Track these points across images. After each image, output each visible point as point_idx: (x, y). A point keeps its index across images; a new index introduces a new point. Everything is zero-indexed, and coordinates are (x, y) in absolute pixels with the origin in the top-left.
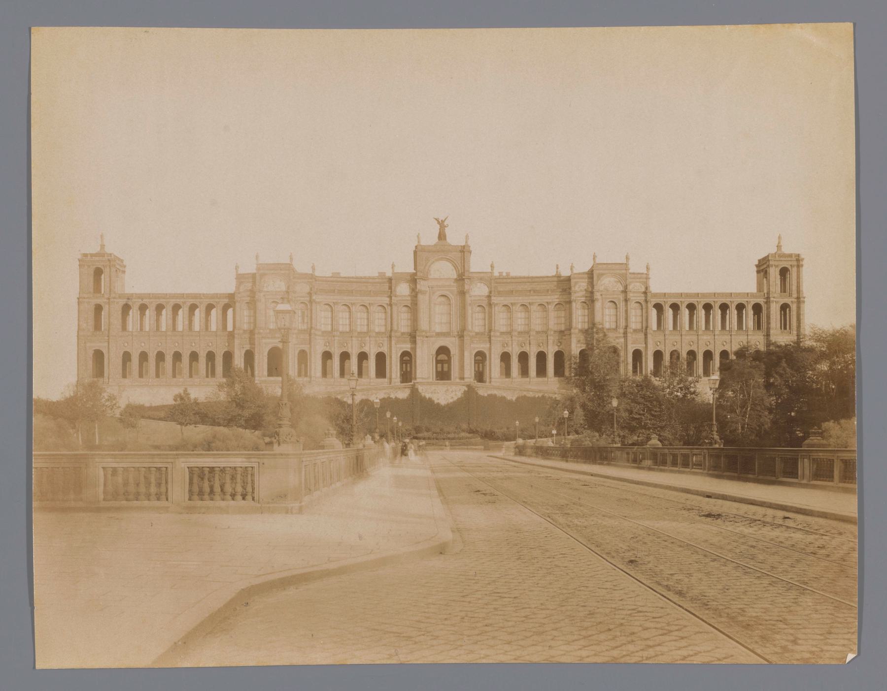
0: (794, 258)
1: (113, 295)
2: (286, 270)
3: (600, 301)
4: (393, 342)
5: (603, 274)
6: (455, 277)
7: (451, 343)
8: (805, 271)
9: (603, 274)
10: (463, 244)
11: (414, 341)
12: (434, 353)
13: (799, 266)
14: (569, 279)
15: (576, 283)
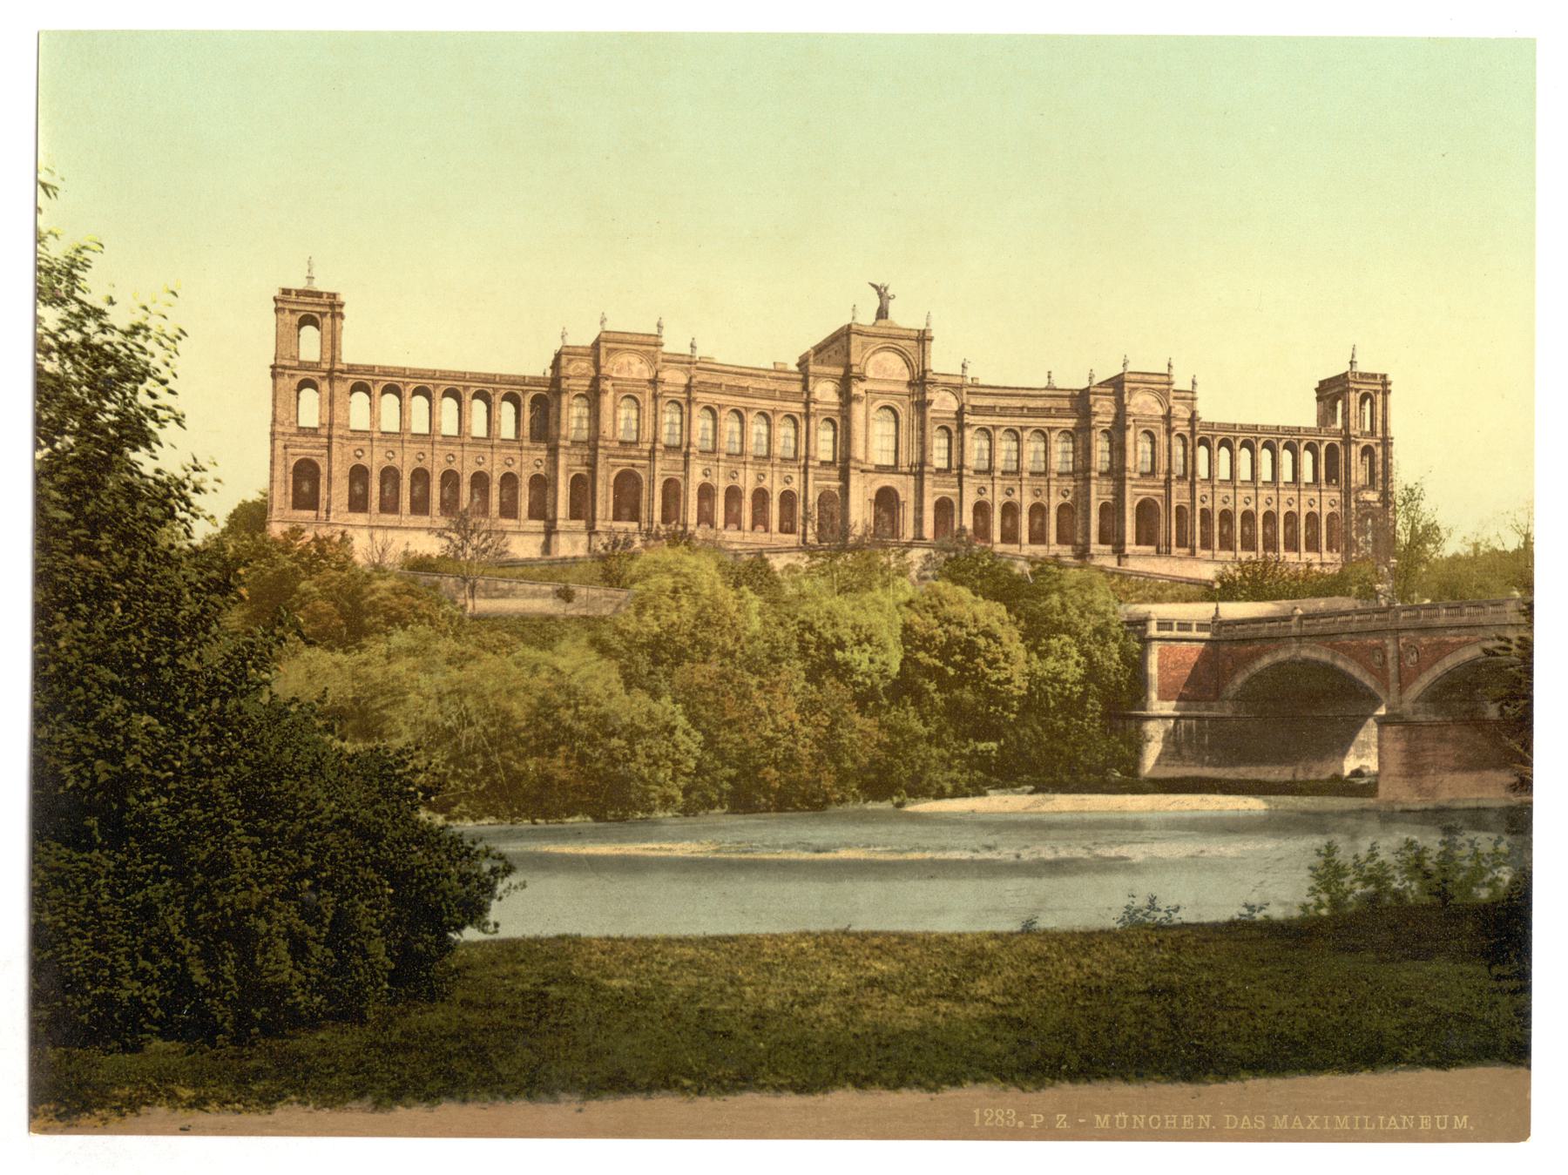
0: (1379, 380)
1: (338, 366)
2: (648, 345)
3: (1132, 429)
4: (811, 476)
5: (1136, 389)
6: (907, 378)
7: (904, 486)
8: (1392, 399)
9: (1136, 389)
10: (923, 327)
11: (844, 477)
12: (873, 497)
13: (1386, 393)
14: (1085, 393)
15: (1096, 400)
